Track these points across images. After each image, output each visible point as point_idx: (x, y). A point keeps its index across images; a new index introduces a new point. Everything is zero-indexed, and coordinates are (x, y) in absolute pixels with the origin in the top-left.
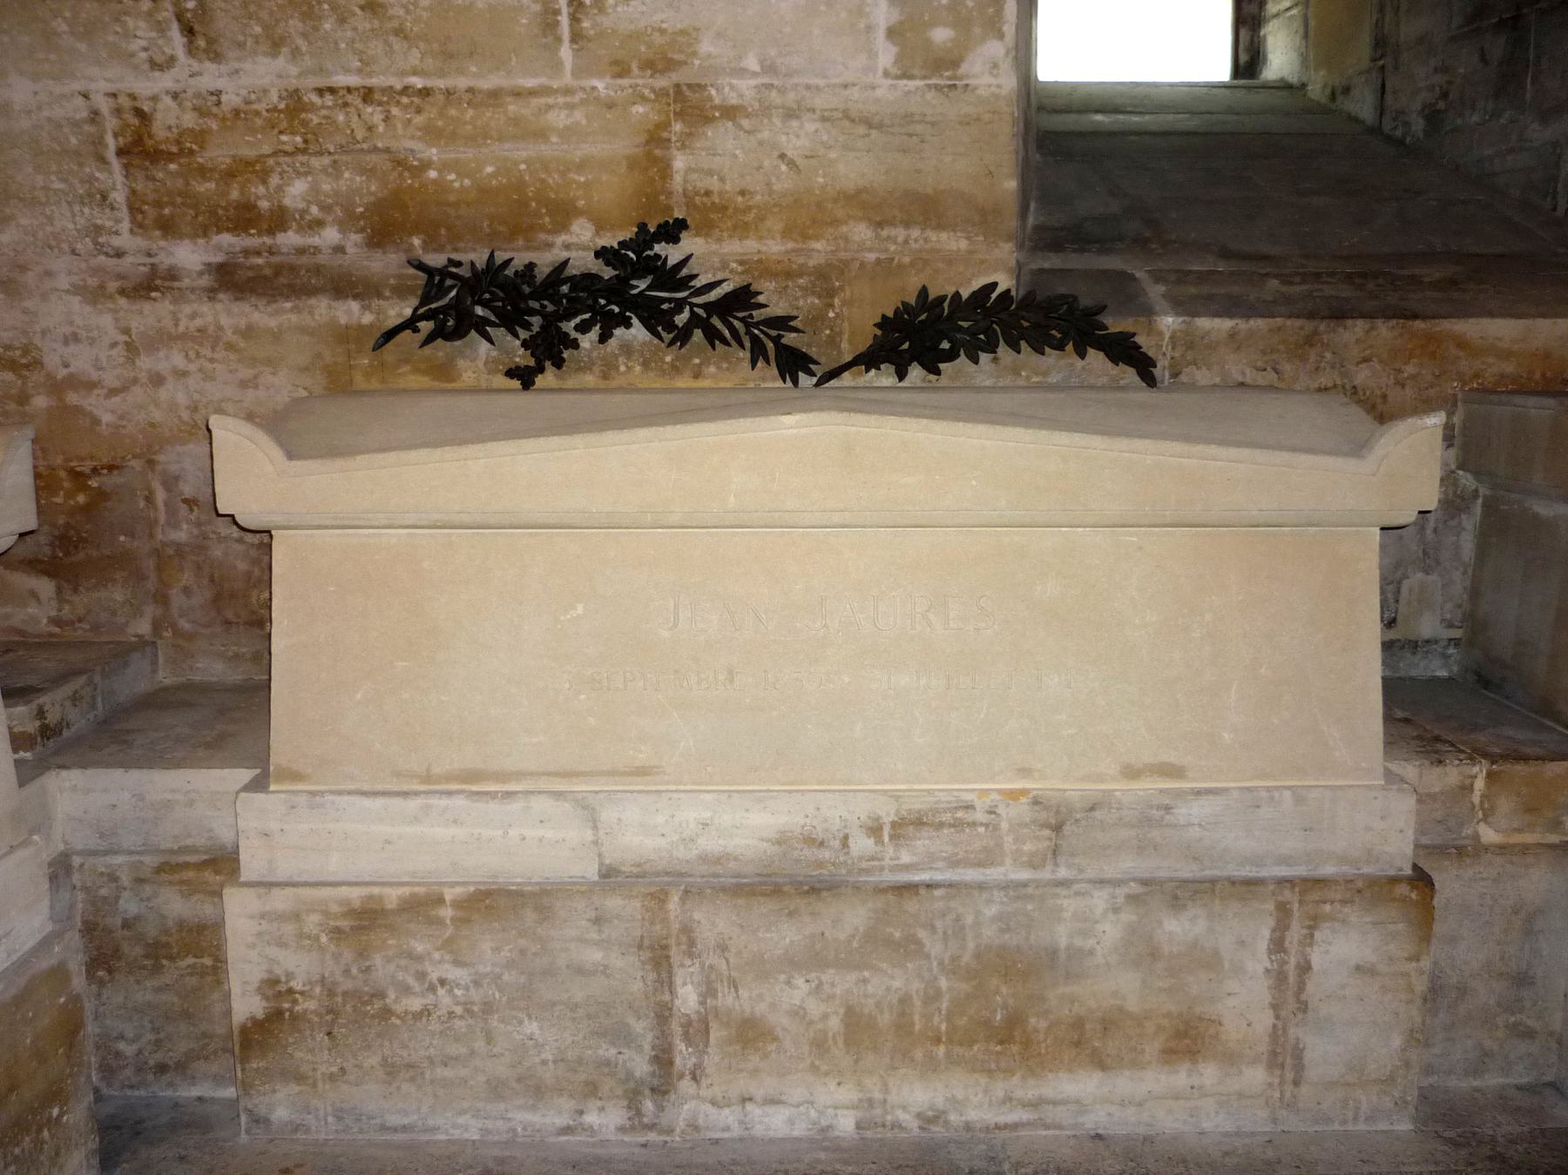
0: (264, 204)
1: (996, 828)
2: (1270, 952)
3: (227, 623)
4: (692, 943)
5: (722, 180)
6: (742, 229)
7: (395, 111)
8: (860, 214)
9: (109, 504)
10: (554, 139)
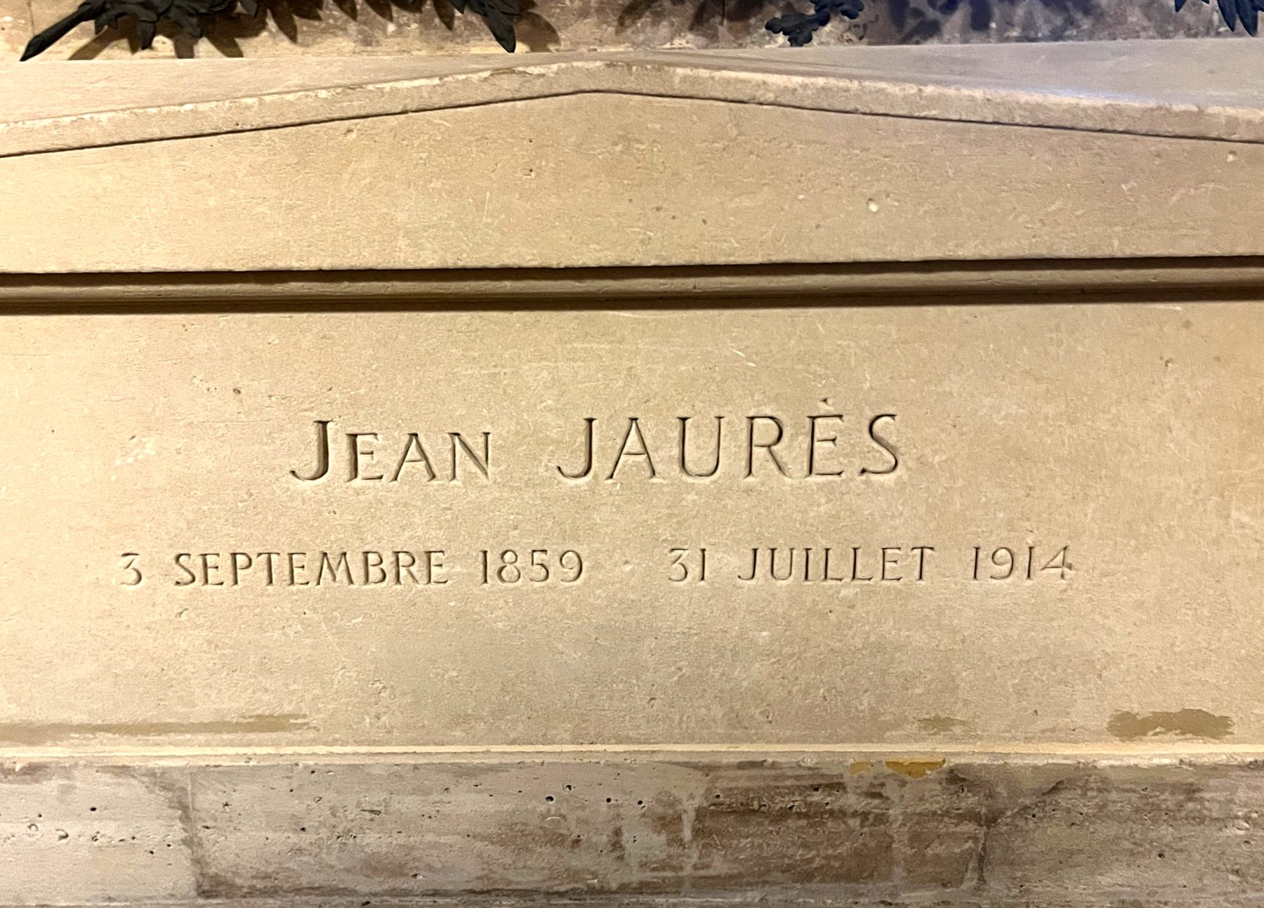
1: (881, 819)
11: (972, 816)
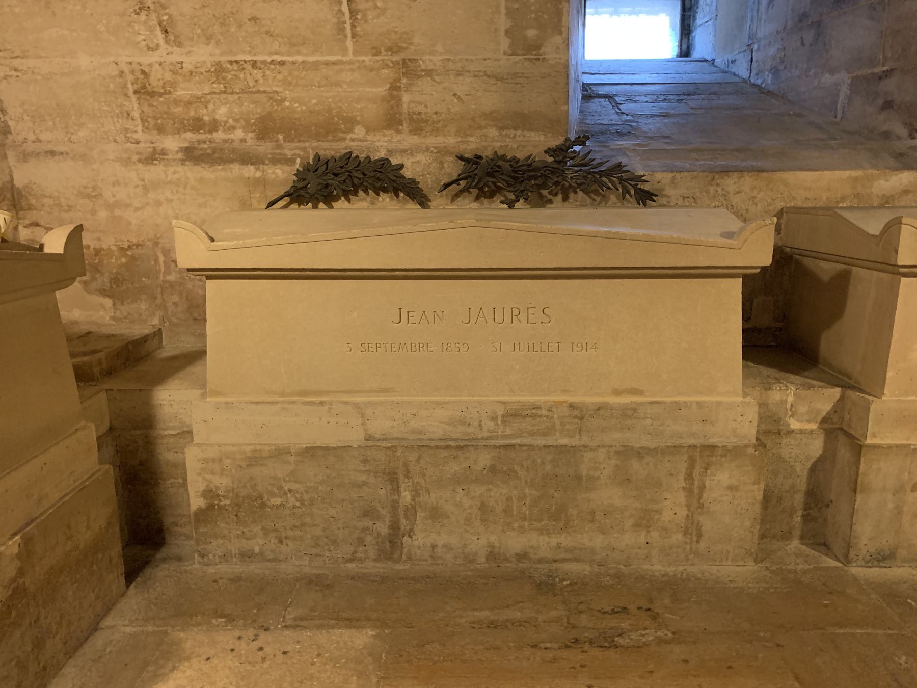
0: (206, 118)
1: (552, 418)
2: (685, 479)
3: (195, 319)
4: (408, 472)
5: (426, 106)
6: (436, 131)
7: (268, 72)
8: (493, 123)
9: (138, 263)
10: (345, 86)
11: (576, 417)
